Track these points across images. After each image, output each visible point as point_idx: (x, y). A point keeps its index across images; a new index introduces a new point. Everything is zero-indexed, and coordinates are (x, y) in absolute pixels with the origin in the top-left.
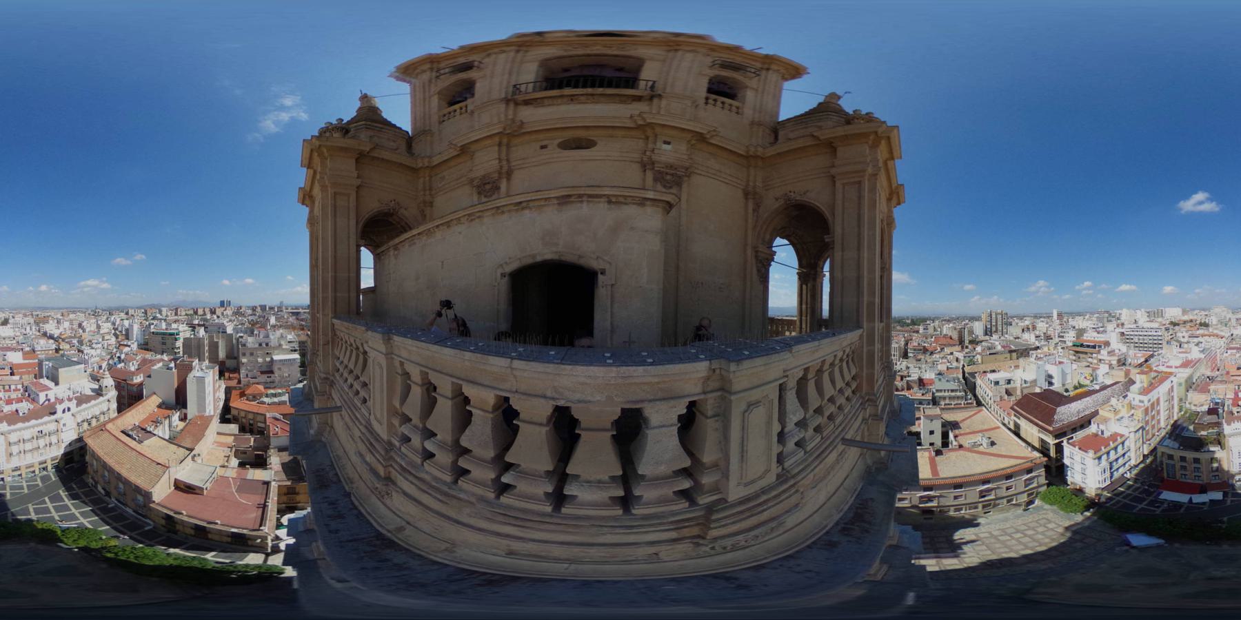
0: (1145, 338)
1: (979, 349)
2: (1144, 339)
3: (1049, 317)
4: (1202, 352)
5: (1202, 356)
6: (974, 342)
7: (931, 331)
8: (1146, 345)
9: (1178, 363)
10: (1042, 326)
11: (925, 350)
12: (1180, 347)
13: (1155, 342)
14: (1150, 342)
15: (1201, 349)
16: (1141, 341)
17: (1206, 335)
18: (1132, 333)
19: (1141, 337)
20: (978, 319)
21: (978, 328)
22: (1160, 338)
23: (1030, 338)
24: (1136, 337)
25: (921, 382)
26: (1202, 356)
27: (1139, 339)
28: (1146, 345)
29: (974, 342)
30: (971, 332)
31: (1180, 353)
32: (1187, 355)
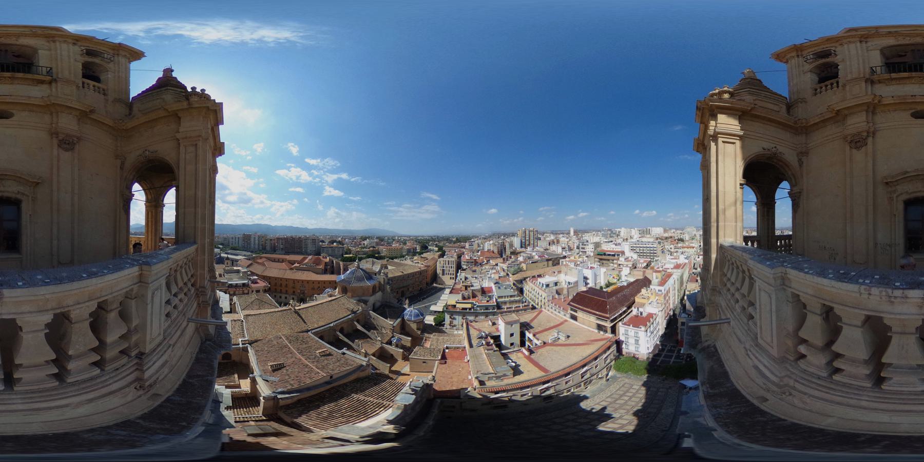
0: (644, 249)
1: (521, 259)
2: (643, 250)
3: (569, 233)
4: (686, 258)
5: (687, 261)
6: (515, 253)
7: (475, 247)
8: (645, 254)
9: (672, 266)
10: (563, 239)
11: (476, 263)
12: (671, 255)
13: (652, 252)
14: (648, 252)
15: (686, 257)
16: (642, 252)
17: (685, 248)
18: (635, 246)
19: (641, 249)
20: (513, 235)
21: (516, 242)
22: (655, 249)
23: (557, 250)
24: (638, 248)
25: (483, 291)
26: (687, 261)
27: (640, 250)
28: (645, 254)
29: (515, 253)
30: (511, 245)
31: (672, 259)
32: (676, 260)
